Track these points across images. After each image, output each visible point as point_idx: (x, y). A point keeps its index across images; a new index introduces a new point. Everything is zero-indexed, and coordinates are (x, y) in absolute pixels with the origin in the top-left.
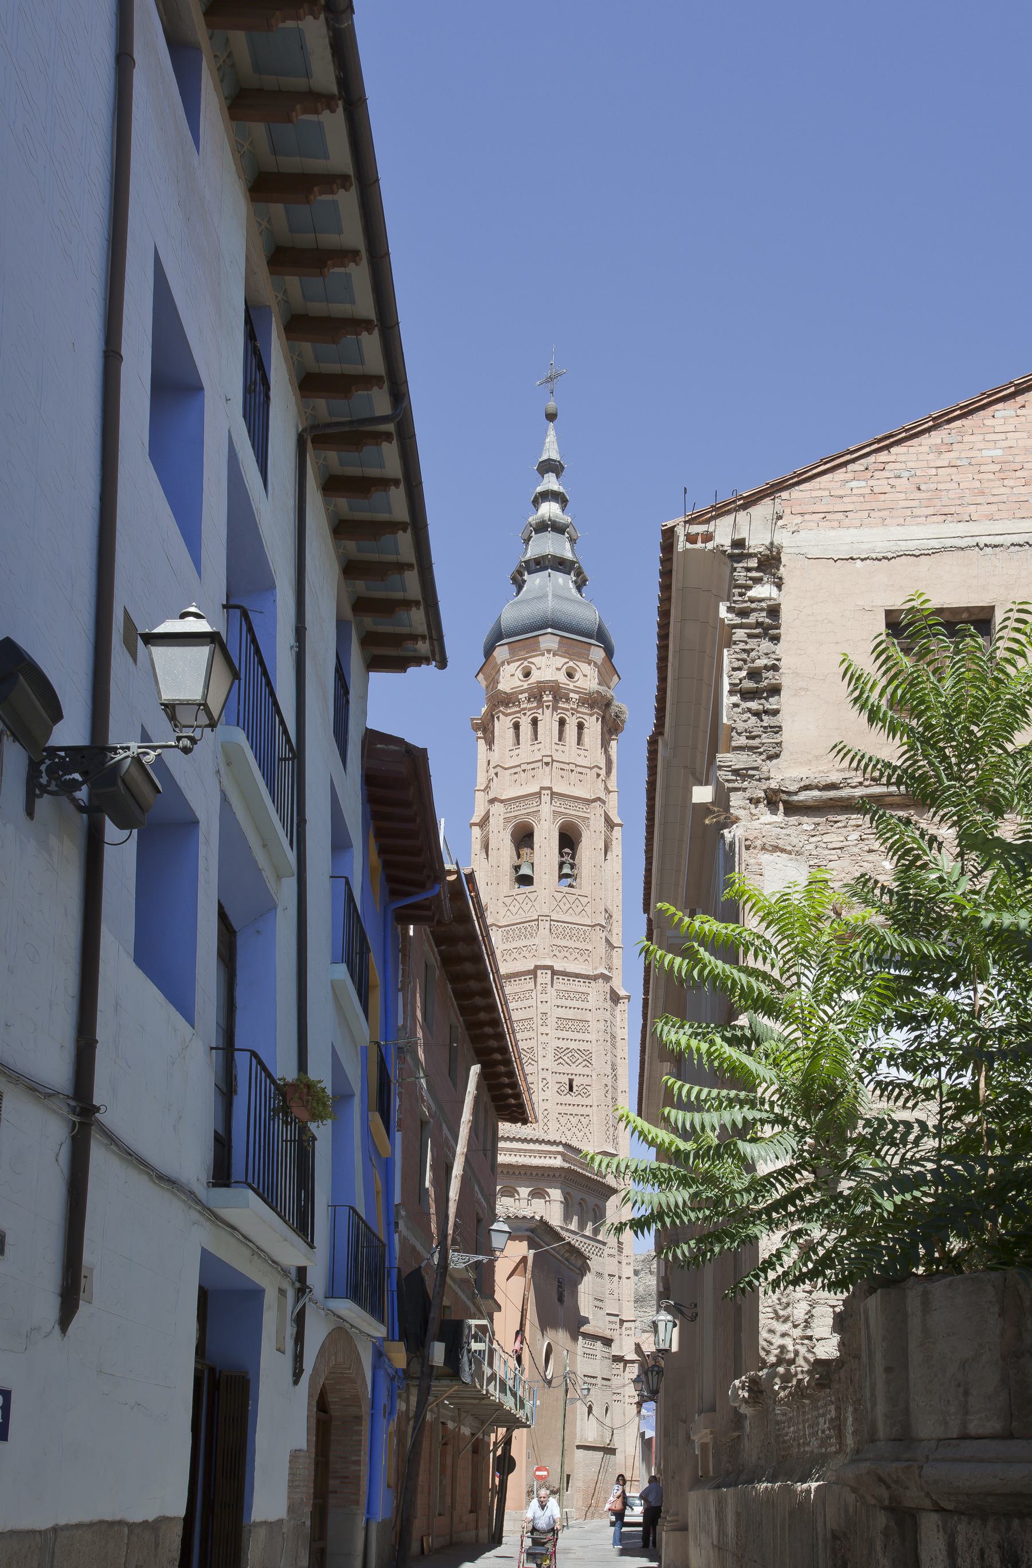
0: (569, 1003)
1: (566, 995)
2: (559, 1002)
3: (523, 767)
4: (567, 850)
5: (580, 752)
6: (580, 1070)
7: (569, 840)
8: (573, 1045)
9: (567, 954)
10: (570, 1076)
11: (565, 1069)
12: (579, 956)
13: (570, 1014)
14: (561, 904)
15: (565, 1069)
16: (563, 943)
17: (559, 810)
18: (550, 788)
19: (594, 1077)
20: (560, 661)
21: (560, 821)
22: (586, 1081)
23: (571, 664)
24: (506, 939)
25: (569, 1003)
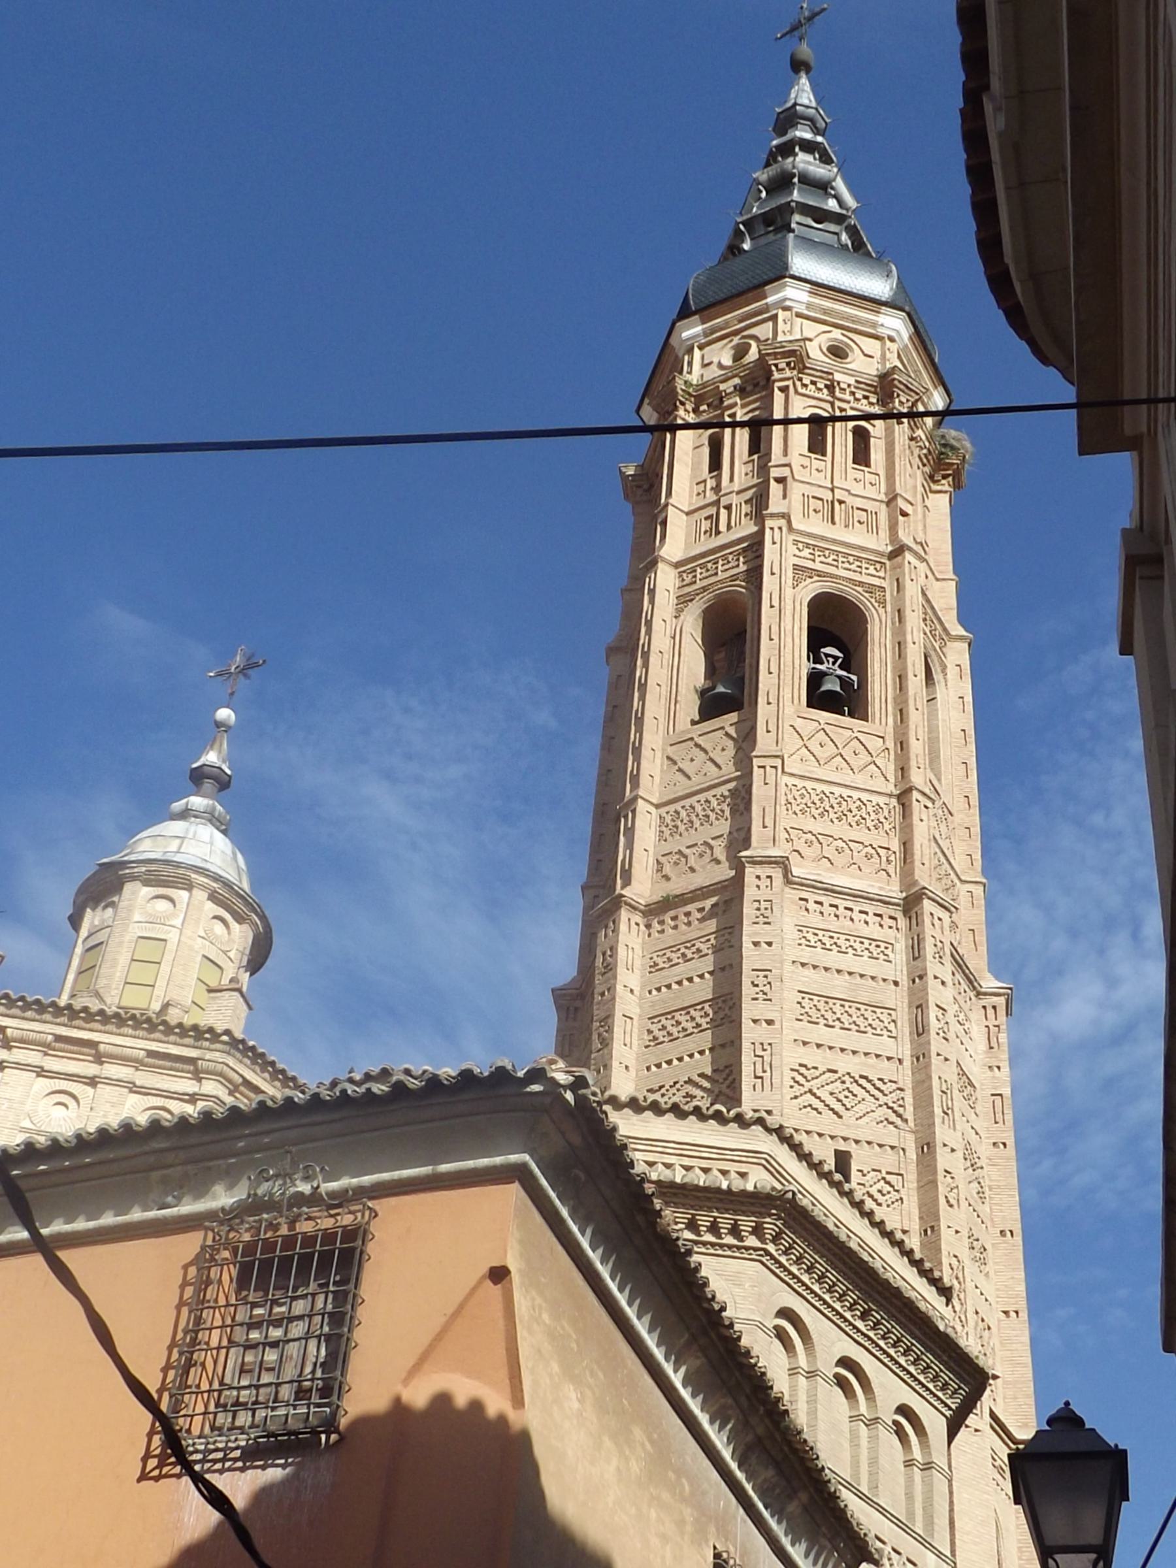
0: (833, 959)
1: (830, 941)
2: (806, 955)
3: (724, 501)
4: (829, 650)
5: (859, 475)
6: (866, 1129)
7: (836, 626)
8: (845, 1064)
9: (829, 852)
10: (842, 1146)
11: (826, 1123)
12: (863, 862)
13: (838, 986)
14: (813, 745)
15: (826, 1123)
16: (818, 826)
17: (809, 564)
18: (786, 516)
19: (912, 1154)
20: (811, 329)
21: (811, 589)
22: (888, 1161)
23: (837, 334)
24: (669, 829)
25: (833, 959)
